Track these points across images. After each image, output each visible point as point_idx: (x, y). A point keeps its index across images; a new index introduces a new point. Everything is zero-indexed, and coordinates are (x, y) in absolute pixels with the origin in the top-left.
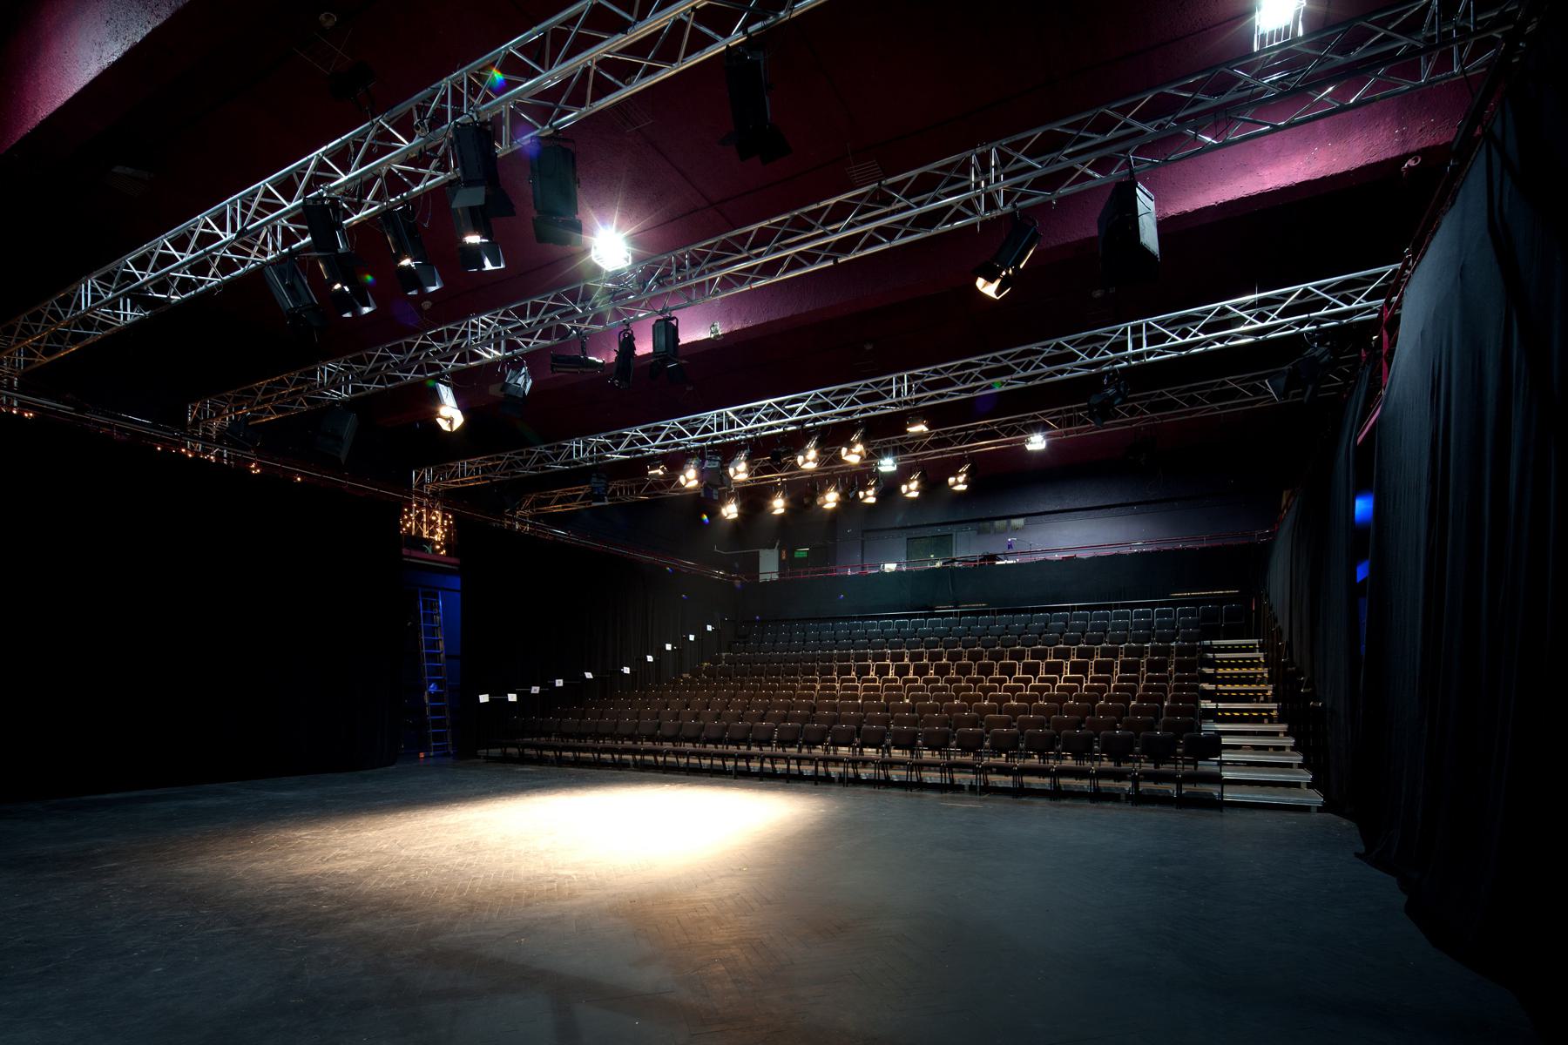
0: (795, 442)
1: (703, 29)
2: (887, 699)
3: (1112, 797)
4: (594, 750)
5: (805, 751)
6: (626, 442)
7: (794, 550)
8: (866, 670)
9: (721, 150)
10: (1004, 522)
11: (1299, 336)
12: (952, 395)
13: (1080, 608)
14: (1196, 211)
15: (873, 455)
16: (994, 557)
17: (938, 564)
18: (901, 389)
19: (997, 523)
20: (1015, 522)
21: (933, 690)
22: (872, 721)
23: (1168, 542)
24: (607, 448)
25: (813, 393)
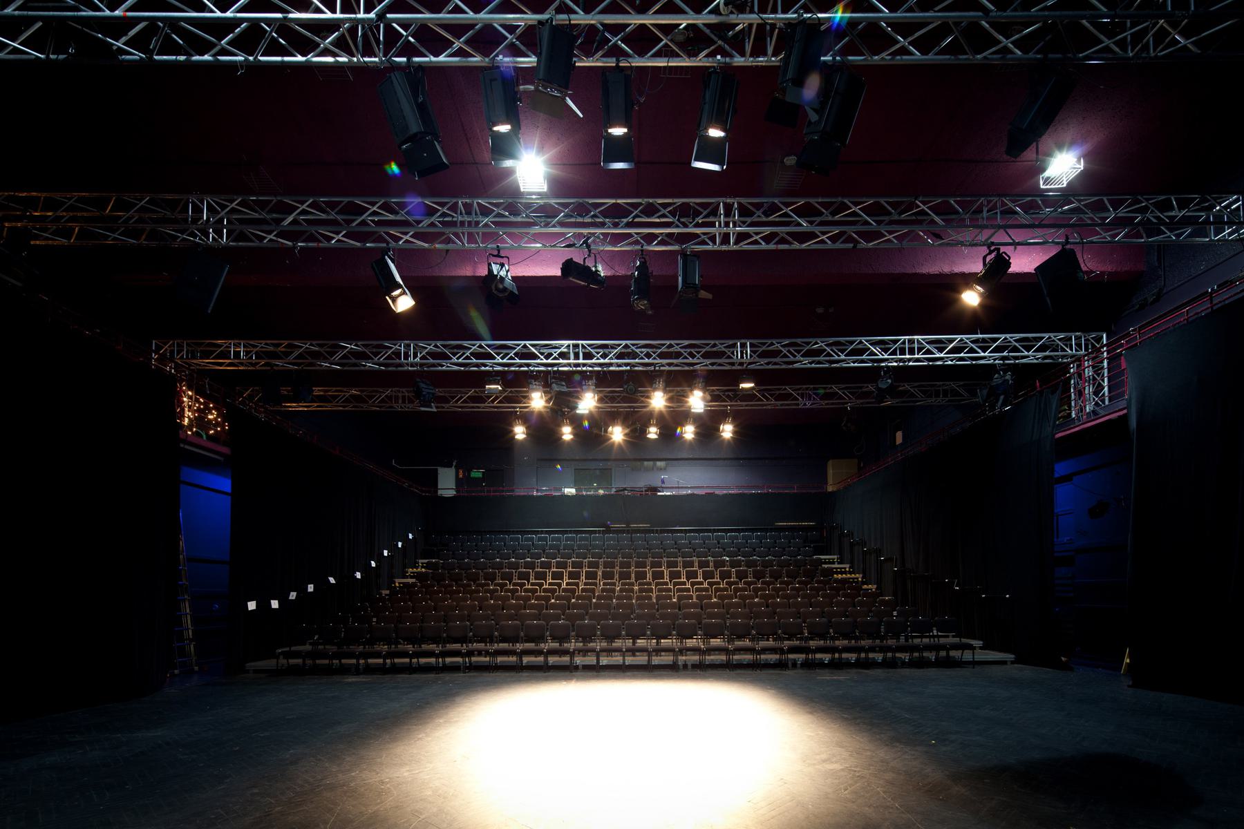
0: (646, 379)
1: (917, 35)
2: (680, 598)
3: (821, 665)
4: (487, 653)
5: (902, 639)
6: (296, 353)
7: (469, 471)
8: (678, 575)
9: (643, 136)
10: (651, 463)
11: (993, 366)
12: (778, 364)
13: (690, 531)
14: (970, 274)
15: (677, 398)
16: (655, 490)
17: (601, 492)
18: (743, 352)
19: (646, 463)
20: (659, 463)
21: (717, 590)
22: (711, 616)
23: (762, 488)
24: (364, 356)
25: (624, 343)
